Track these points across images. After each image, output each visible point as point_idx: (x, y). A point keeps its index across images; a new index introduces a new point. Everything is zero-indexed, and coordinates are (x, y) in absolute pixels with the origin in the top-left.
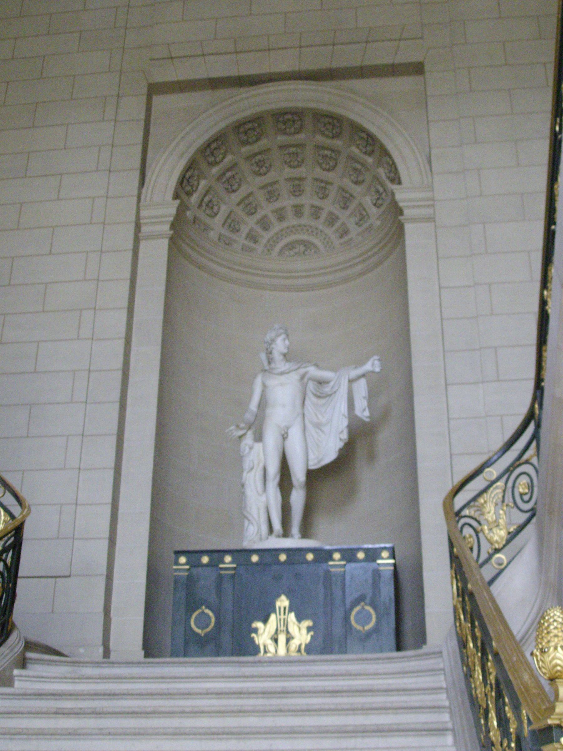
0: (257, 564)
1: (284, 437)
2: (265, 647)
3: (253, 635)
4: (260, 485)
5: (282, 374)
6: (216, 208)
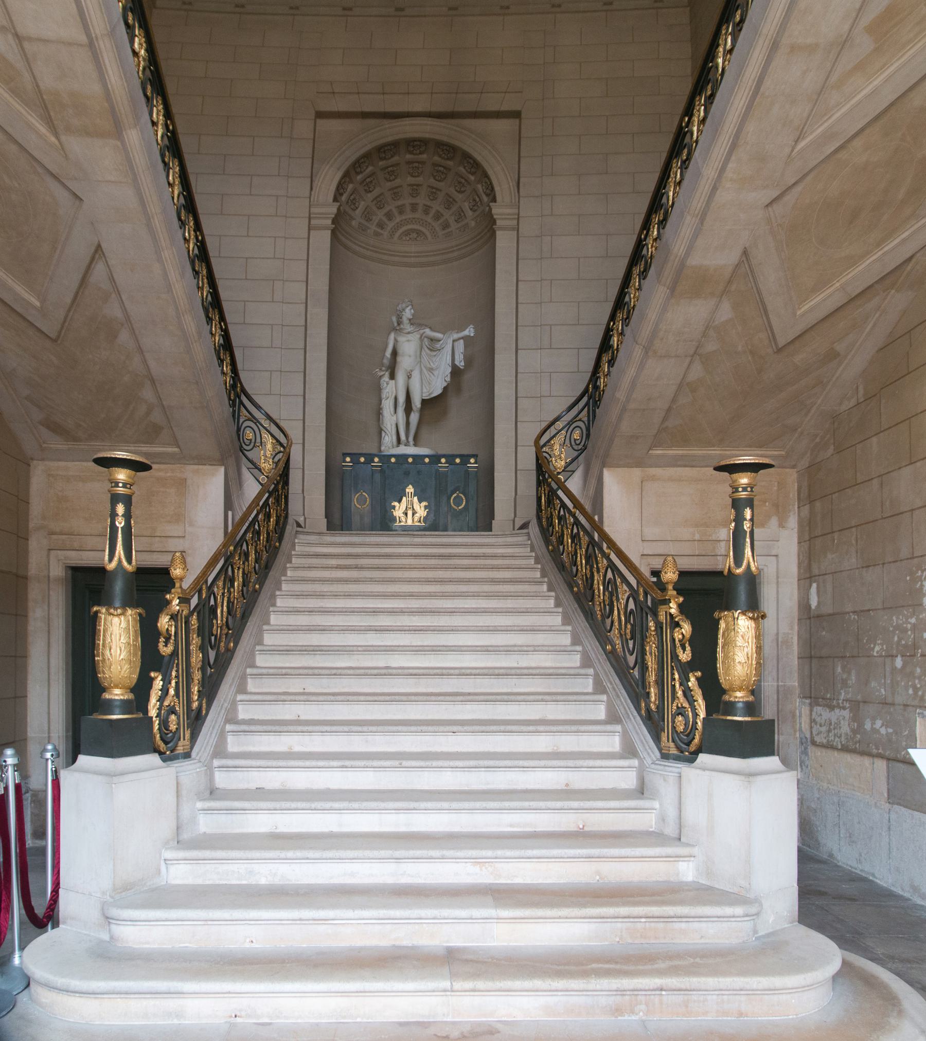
0: (394, 463)
1: (409, 377)
4: (392, 409)
5: (409, 333)
6: (357, 203)
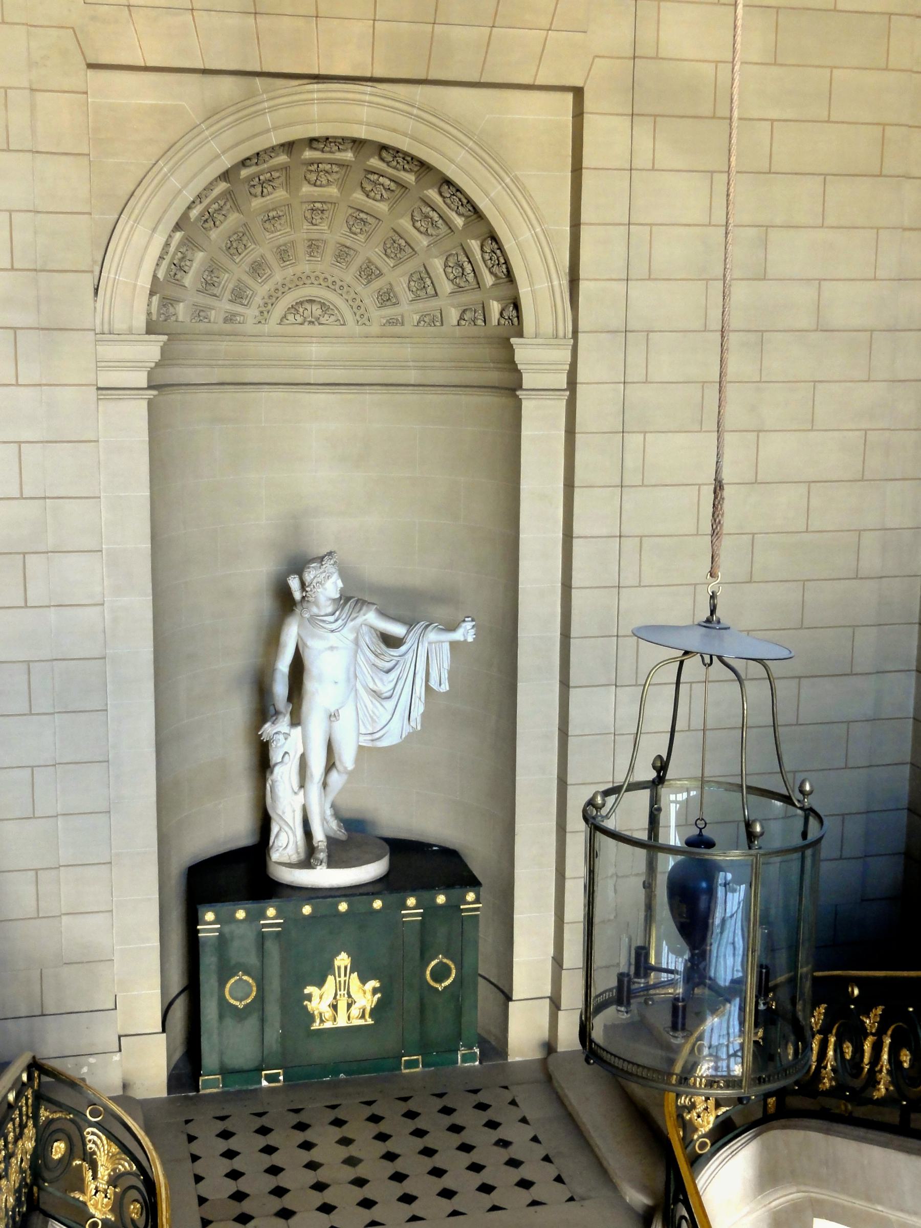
2: (321, 1014)
3: (306, 1003)
